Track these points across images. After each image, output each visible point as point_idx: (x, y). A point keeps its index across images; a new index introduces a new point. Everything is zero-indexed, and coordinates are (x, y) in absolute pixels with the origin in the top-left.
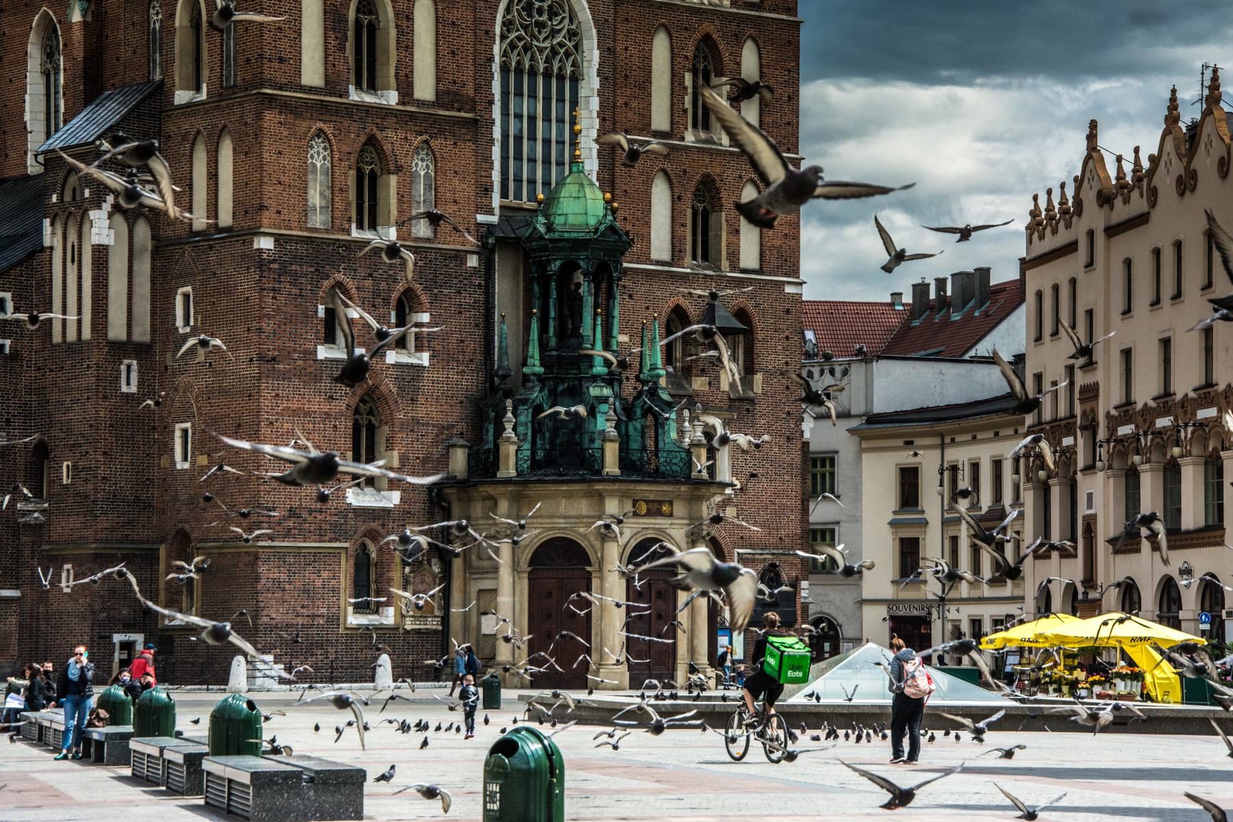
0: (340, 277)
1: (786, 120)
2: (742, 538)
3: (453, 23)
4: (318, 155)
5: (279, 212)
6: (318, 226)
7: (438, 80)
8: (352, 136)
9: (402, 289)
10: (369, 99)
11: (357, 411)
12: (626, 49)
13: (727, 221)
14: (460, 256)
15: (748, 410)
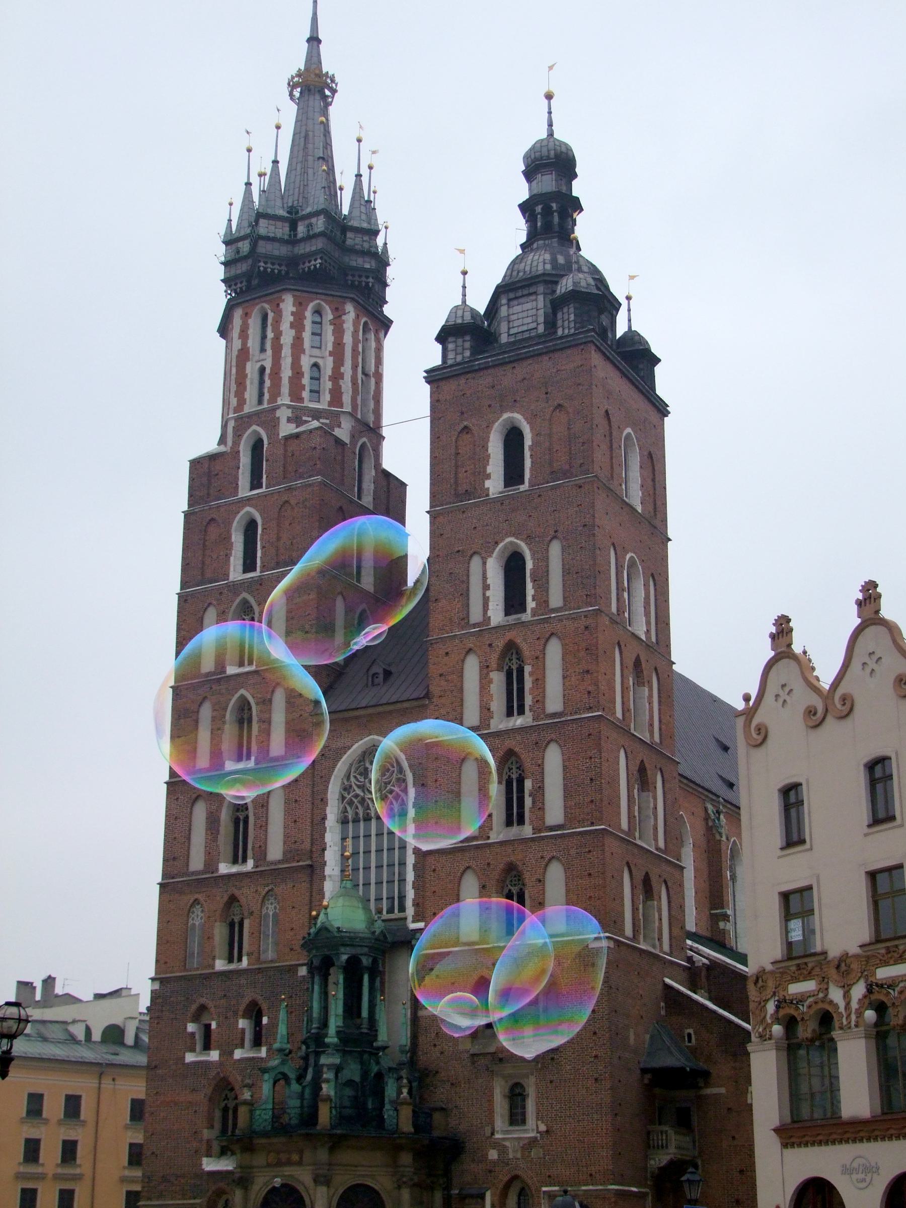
0: (203, 1000)
1: (588, 799)
2: (549, 1176)
3: (296, 801)
4: (198, 915)
5: (166, 963)
6: (195, 966)
7: (285, 843)
8: (218, 898)
9: (247, 1002)
10: (235, 869)
11: (226, 1098)
12: (436, 781)
13: (530, 897)
14: (293, 969)
15: (553, 1059)
